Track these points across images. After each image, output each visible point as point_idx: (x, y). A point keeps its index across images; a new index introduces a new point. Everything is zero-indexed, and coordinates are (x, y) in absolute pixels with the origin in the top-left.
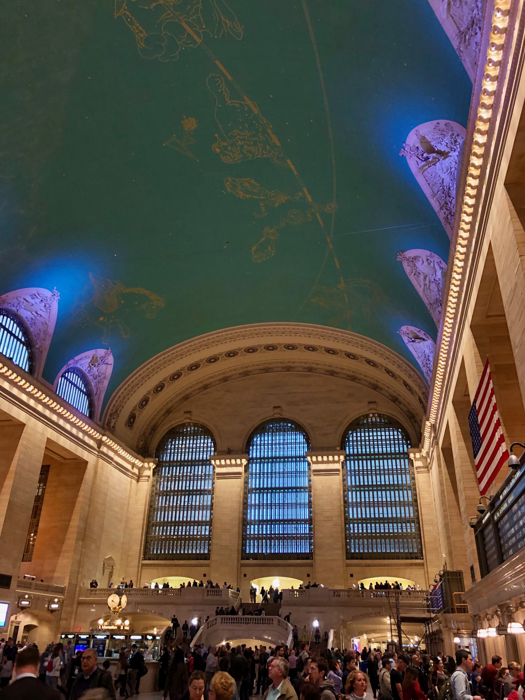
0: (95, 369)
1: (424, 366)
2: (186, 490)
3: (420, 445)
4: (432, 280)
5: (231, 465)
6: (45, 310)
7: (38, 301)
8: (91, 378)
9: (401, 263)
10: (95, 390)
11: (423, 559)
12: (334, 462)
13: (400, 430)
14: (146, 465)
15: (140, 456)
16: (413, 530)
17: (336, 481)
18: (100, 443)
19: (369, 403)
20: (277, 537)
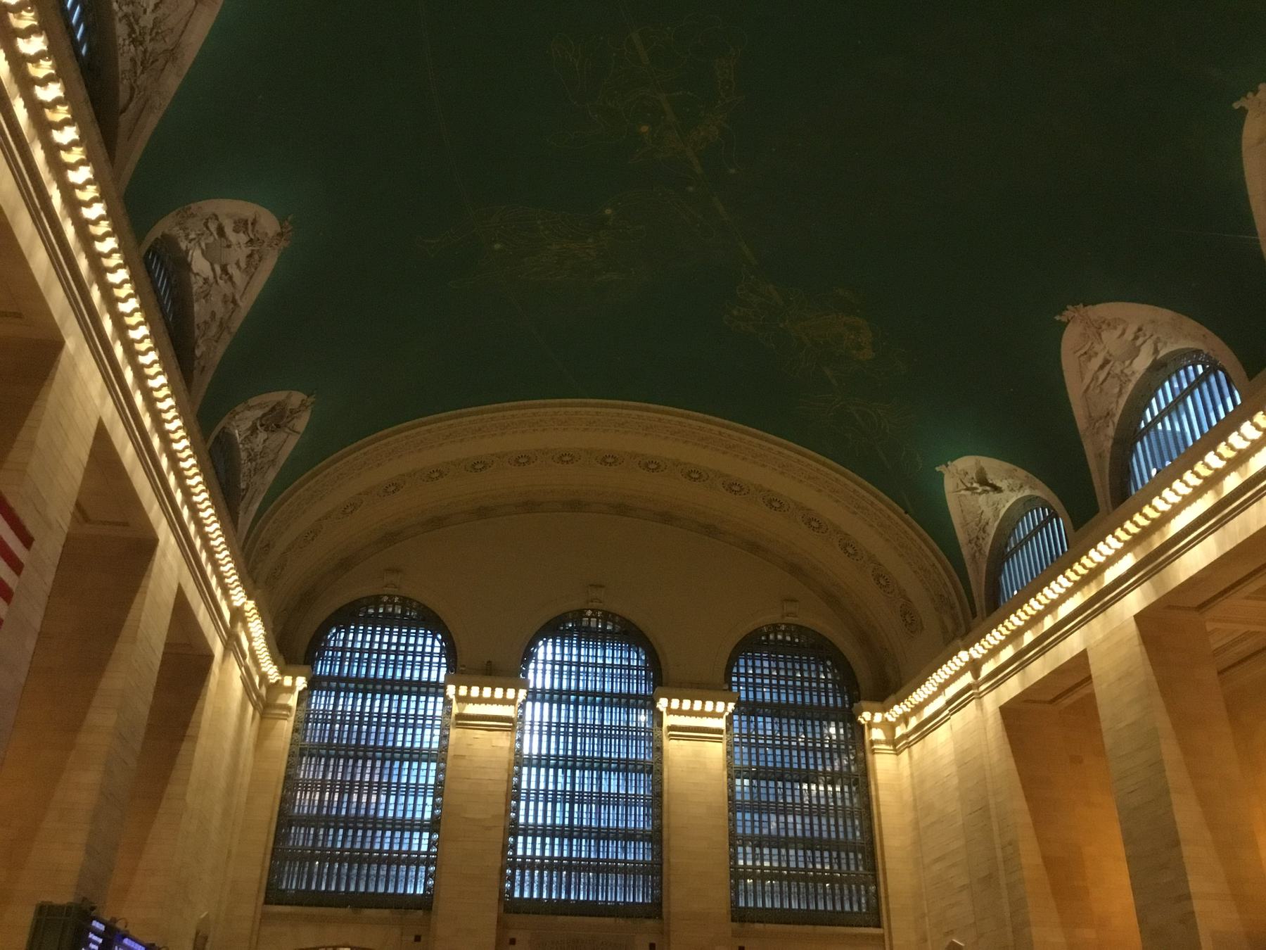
0: (262, 435)
1: (970, 542)
2: (375, 747)
3: (892, 698)
4: (1118, 371)
5: (492, 701)
6: (243, 265)
7: (243, 238)
8: (244, 455)
9: (1063, 326)
10: (243, 486)
11: (878, 925)
12: (713, 715)
13: (829, 663)
14: (288, 681)
15: (281, 659)
16: (861, 869)
17: (715, 752)
18: (238, 614)
19: (786, 600)
20: (612, 868)
